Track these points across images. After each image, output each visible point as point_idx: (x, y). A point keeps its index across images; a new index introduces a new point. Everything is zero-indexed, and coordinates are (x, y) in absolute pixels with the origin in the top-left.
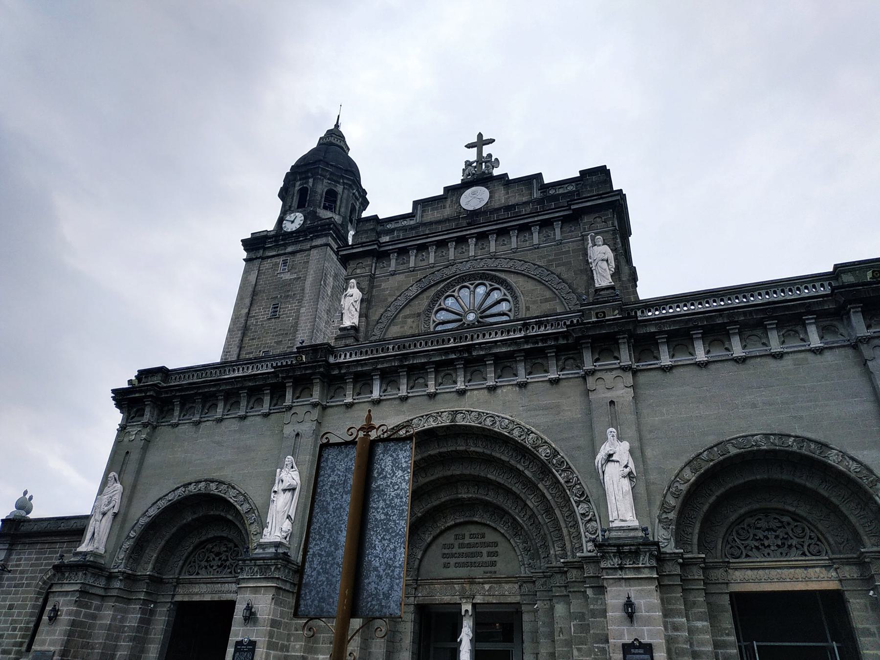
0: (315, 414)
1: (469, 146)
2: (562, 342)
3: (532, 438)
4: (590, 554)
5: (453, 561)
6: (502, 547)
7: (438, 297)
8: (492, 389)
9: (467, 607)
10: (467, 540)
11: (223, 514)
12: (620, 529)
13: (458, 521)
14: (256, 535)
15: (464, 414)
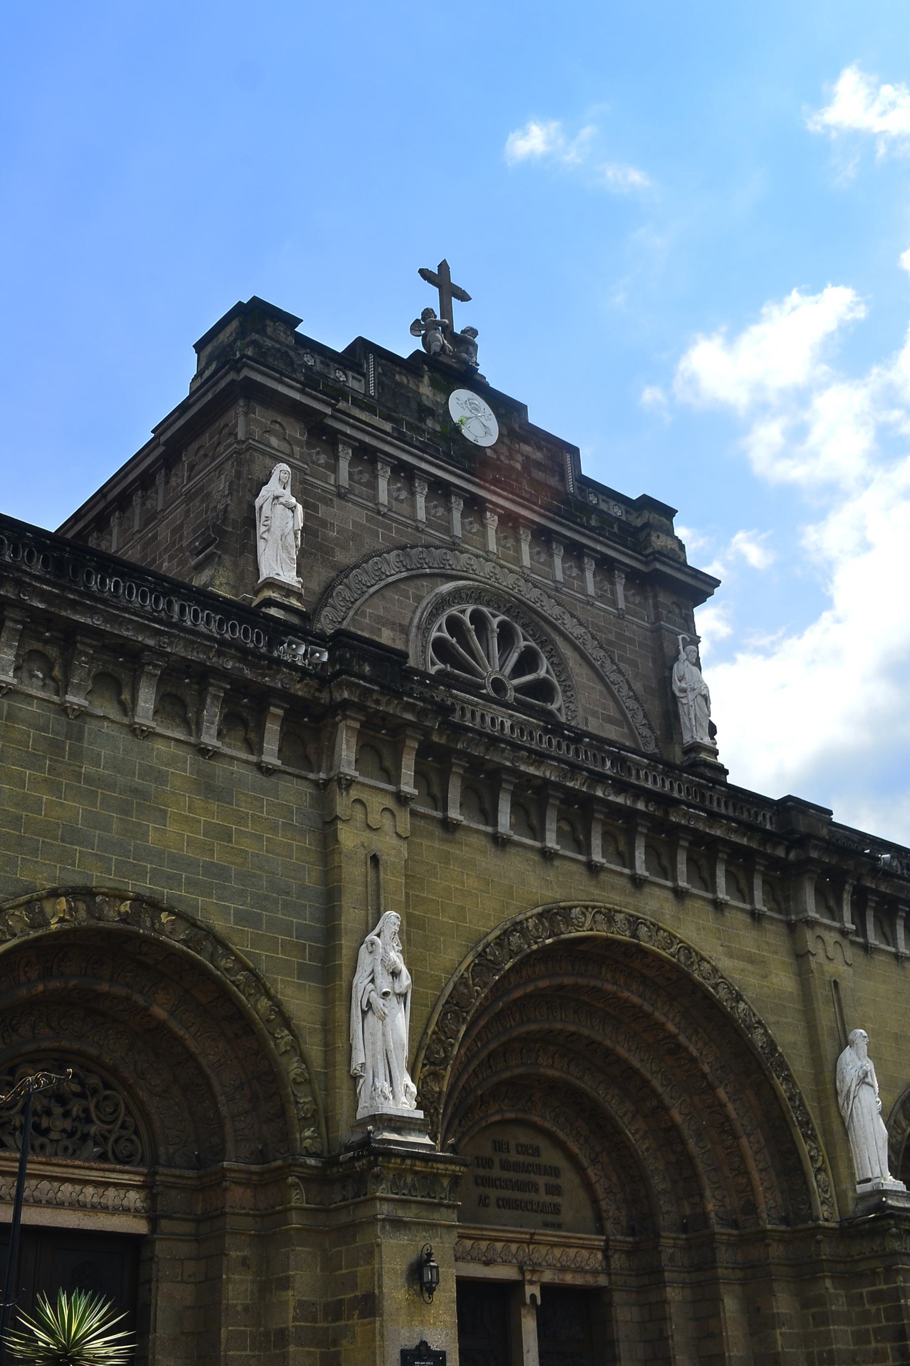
0: (404, 821)
1: (425, 274)
2: (780, 852)
3: (744, 1010)
4: (826, 1224)
5: (493, 1194)
6: (569, 1179)
7: (436, 609)
8: (680, 895)
9: (532, 1290)
10: (513, 1157)
11: (140, 1000)
12: (895, 1194)
13: (511, 1115)
14: (300, 1083)
15: (648, 927)
